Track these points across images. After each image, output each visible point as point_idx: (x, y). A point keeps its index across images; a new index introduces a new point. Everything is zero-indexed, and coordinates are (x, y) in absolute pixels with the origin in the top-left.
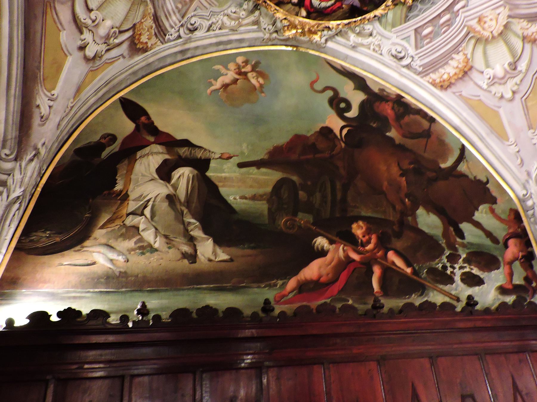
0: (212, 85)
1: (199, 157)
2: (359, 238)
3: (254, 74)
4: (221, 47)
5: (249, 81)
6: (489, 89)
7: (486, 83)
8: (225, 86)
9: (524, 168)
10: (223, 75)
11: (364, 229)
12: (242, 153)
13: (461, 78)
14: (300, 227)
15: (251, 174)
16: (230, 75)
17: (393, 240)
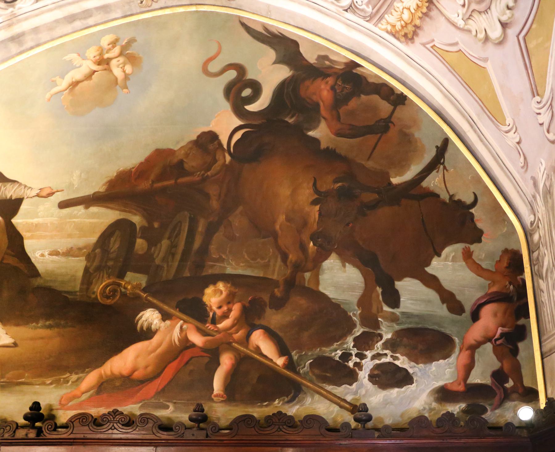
0: (56, 85)
1: (8, 197)
2: (211, 309)
3: (121, 59)
4: (78, 24)
5: (111, 71)
6: (466, 27)
7: (461, 16)
8: (75, 84)
9: (528, 175)
10: (75, 68)
11: (224, 294)
12: (71, 185)
13: (426, 14)
14: (124, 295)
15: (75, 217)
16: (88, 65)
17: (268, 311)
